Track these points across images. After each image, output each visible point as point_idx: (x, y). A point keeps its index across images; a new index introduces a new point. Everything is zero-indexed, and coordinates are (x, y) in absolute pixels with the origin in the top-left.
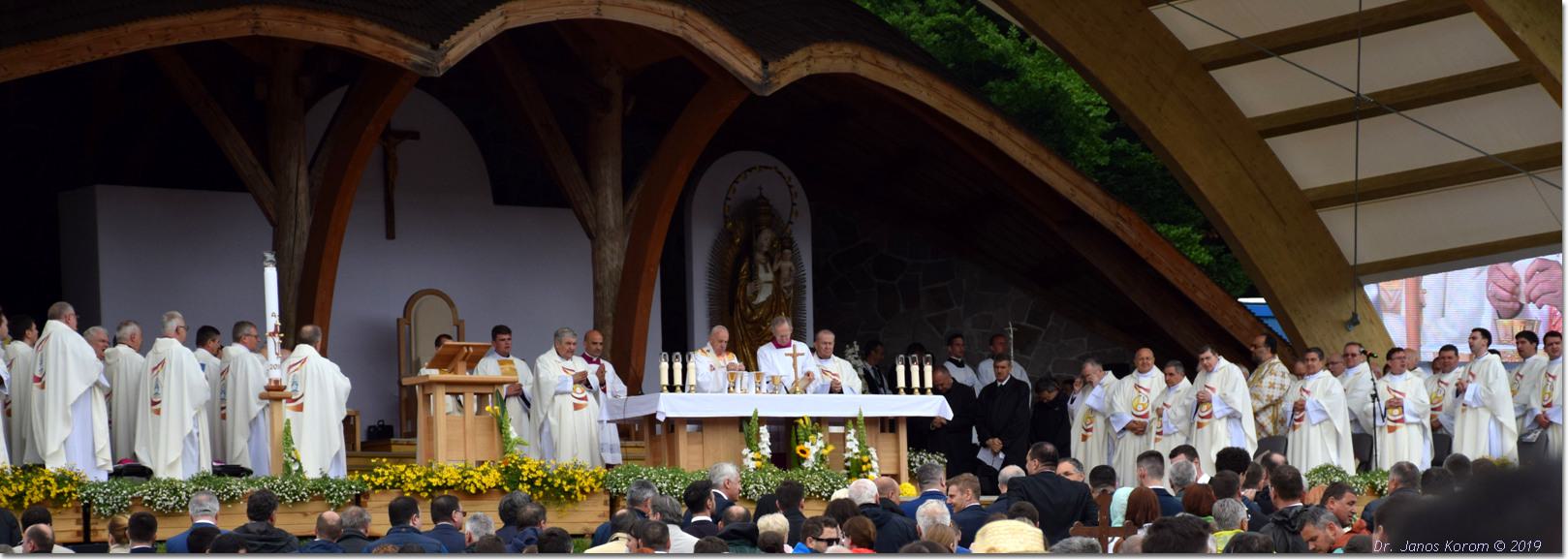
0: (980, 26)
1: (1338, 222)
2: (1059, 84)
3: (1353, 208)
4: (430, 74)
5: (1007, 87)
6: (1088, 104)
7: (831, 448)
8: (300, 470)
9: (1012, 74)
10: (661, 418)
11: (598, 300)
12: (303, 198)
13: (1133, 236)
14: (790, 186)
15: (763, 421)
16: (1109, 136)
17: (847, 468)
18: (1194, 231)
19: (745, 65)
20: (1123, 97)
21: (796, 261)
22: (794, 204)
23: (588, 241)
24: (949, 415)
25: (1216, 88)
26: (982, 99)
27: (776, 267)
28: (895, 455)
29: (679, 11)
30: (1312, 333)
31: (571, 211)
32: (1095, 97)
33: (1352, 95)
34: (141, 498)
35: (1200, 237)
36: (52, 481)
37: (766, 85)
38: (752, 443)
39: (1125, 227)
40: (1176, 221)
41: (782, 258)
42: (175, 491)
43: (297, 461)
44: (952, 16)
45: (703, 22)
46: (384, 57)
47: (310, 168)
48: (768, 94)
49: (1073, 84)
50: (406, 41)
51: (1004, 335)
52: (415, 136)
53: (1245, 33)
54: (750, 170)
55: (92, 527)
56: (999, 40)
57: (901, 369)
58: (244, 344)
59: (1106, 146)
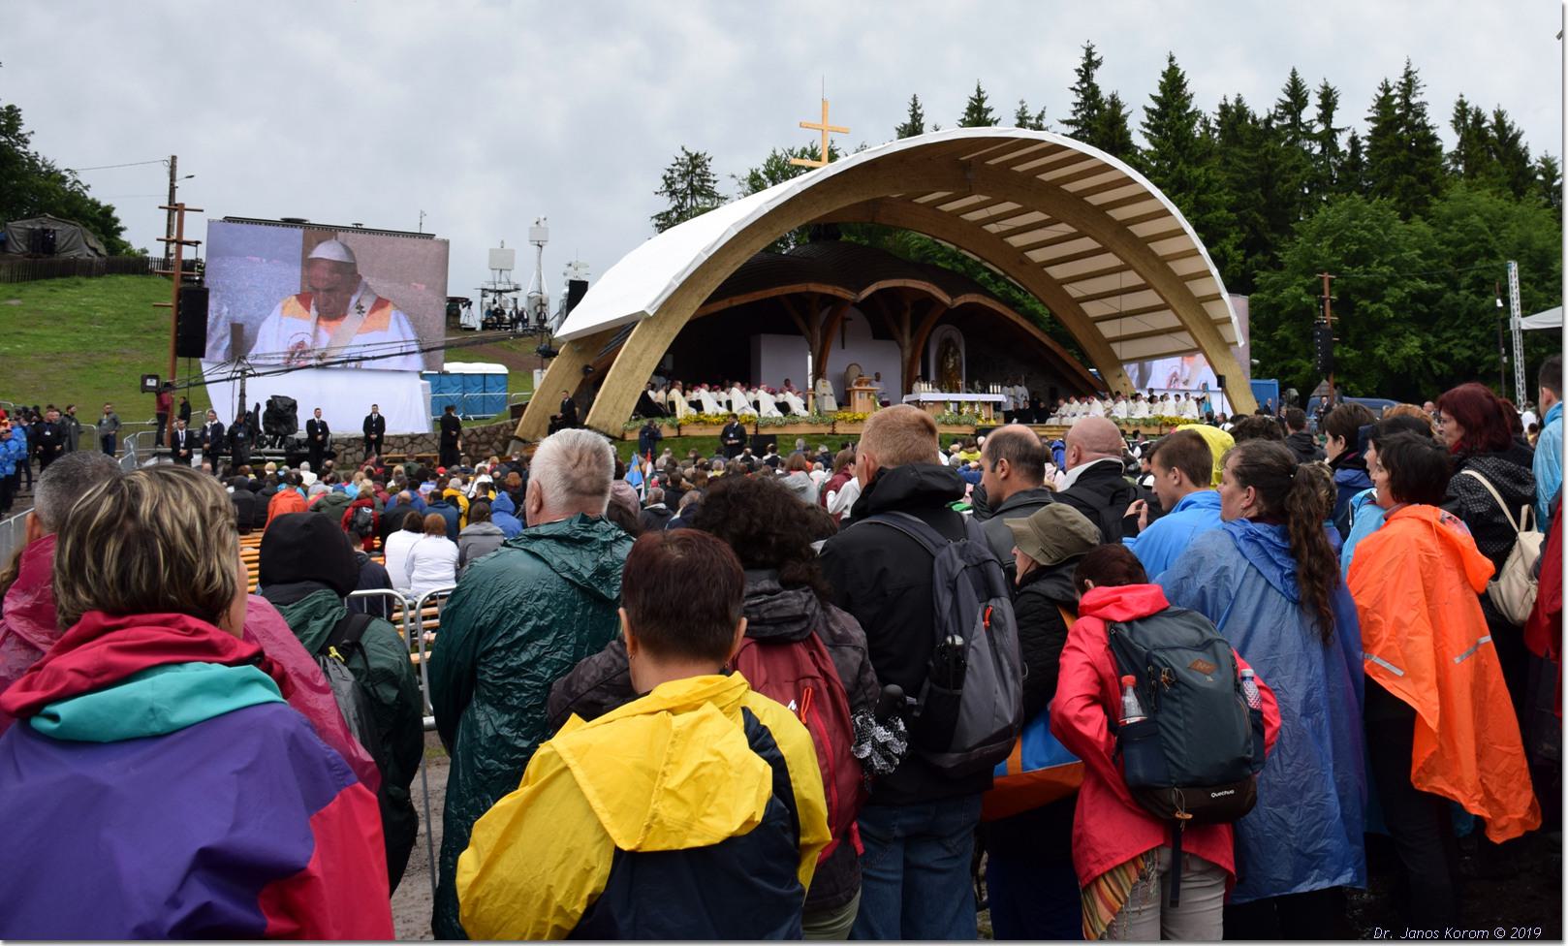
1: (1115, 347)
9: (1022, 305)
16: (1050, 323)
19: (946, 299)
26: (1016, 311)
32: (1047, 311)
38: (948, 408)
49: (1040, 308)
53: (1089, 293)
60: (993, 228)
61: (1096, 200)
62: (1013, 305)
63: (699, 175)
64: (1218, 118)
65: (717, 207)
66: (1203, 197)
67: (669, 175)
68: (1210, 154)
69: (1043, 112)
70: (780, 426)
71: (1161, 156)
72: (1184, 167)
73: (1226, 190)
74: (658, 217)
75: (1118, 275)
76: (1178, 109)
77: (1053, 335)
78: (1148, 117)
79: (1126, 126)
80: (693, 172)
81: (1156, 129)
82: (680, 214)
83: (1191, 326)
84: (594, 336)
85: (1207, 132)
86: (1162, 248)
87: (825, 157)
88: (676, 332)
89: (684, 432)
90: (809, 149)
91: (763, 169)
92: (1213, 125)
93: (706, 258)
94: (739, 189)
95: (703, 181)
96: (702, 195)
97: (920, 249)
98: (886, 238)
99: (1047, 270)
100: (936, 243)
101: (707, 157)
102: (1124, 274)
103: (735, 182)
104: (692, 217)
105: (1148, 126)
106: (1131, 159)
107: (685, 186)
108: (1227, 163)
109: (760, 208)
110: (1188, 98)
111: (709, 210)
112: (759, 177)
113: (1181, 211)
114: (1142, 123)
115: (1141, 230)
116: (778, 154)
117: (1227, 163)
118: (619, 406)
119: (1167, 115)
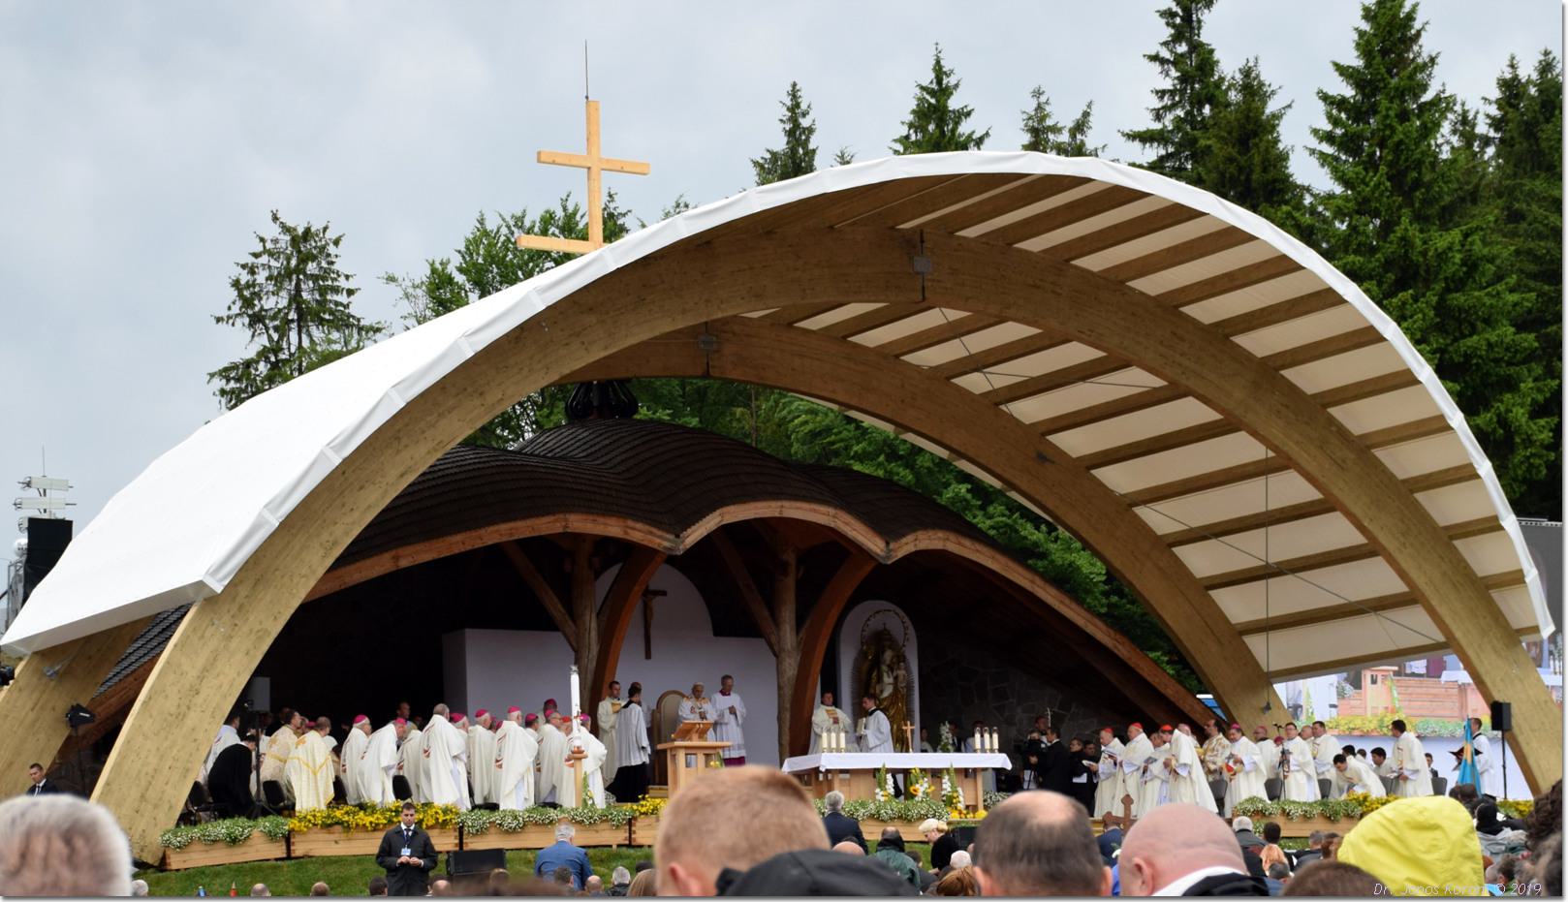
0: (1022, 525)
1: (1256, 644)
2: (1074, 562)
3: (1265, 636)
4: (674, 553)
5: (1040, 564)
6: (1091, 573)
7: (933, 788)
8: (594, 803)
9: (1043, 556)
10: (823, 769)
11: (780, 696)
12: (594, 634)
13: (1125, 653)
14: (903, 623)
15: (888, 771)
16: (1106, 594)
17: (943, 801)
18: (1164, 654)
19: (874, 544)
20: (1117, 564)
21: (908, 669)
22: (906, 634)
23: (774, 658)
24: (1009, 766)
25: (1177, 560)
27: (895, 674)
28: (974, 793)
29: (832, 511)
30: (1243, 714)
31: (763, 640)
33: (1264, 563)
34: (494, 822)
35: (1166, 659)
36: (440, 812)
37: (888, 558)
38: (882, 785)
39: (1120, 647)
40: (1153, 649)
41: (899, 668)
42: (516, 818)
43: (591, 798)
44: (1004, 519)
45: (848, 518)
46: (646, 543)
47: (598, 615)
48: (889, 562)
50: (659, 533)
51: (1044, 716)
52: (664, 593)
53: (1195, 524)
54: (878, 612)
55: (465, 841)
56: (1034, 534)
57: (978, 736)
58: (553, 724)
59: (1104, 601)
60: (975, 383)
61: (1208, 312)
62: (1025, 554)
63: (315, 278)
64: (1494, 111)
65: (357, 349)
66: (1458, 299)
67: (245, 277)
68: (1474, 197)
69: (1086, 114)
70: (511, 832)
71: (1362, 207)
72: (1414, 232)
73: (1513, 280)
74: (224, 373)
75: (1260, 482)
76: (1401, 94)
77: (1112, 619)
78: (1329, 116)
79: (1276, 141)
80: (299, 270)
81: (1349, 143)
82: (275, 366)
83: (1428, 591)
84: (88, 640)
85: (1469, 145)
86: (1361, 418)
87: (597, 231)
88: (276, 629)
89: (299, 849)
90: (560, 214)
91: (456, 260)
92: (1482, 128)
93: (337, 461)
94: (406, 308)
95: (323, 291)
96: (321, 322)
97: (815, 435)
98: (739, 411)
99: (1096, 472)
100: (850, 420)
101: (331, 235)
102: (1275, 479)
103: (395, 291)
104: (301, 373)
105: (1329, 138)
106: (1289, 215)
107: (283, 302)
108: (1515, 217)
109: (454, 347)
110: (1425, 66)
111: (339, 355)
112: (450, 280)
113: (1407, 331)
114: (1315, 132)
115: (1314, 378)
116: (491, 225)
117: (1515, 217)
118: (151, 794)
119: (1374, 110)
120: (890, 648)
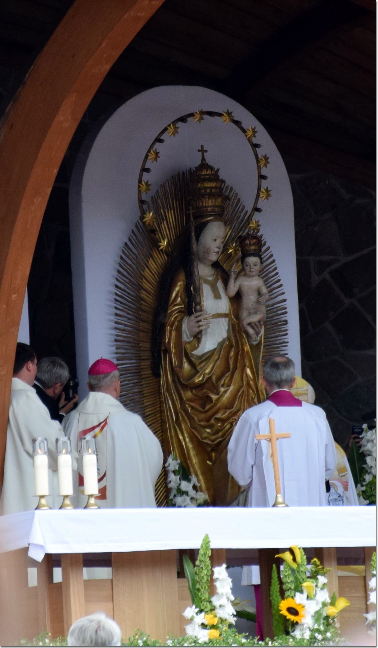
7: (342, 603)
14: (255, 146)
27: (233, 288)
41: (242, 272)
54: (183, 119)
120: (220, 215)
